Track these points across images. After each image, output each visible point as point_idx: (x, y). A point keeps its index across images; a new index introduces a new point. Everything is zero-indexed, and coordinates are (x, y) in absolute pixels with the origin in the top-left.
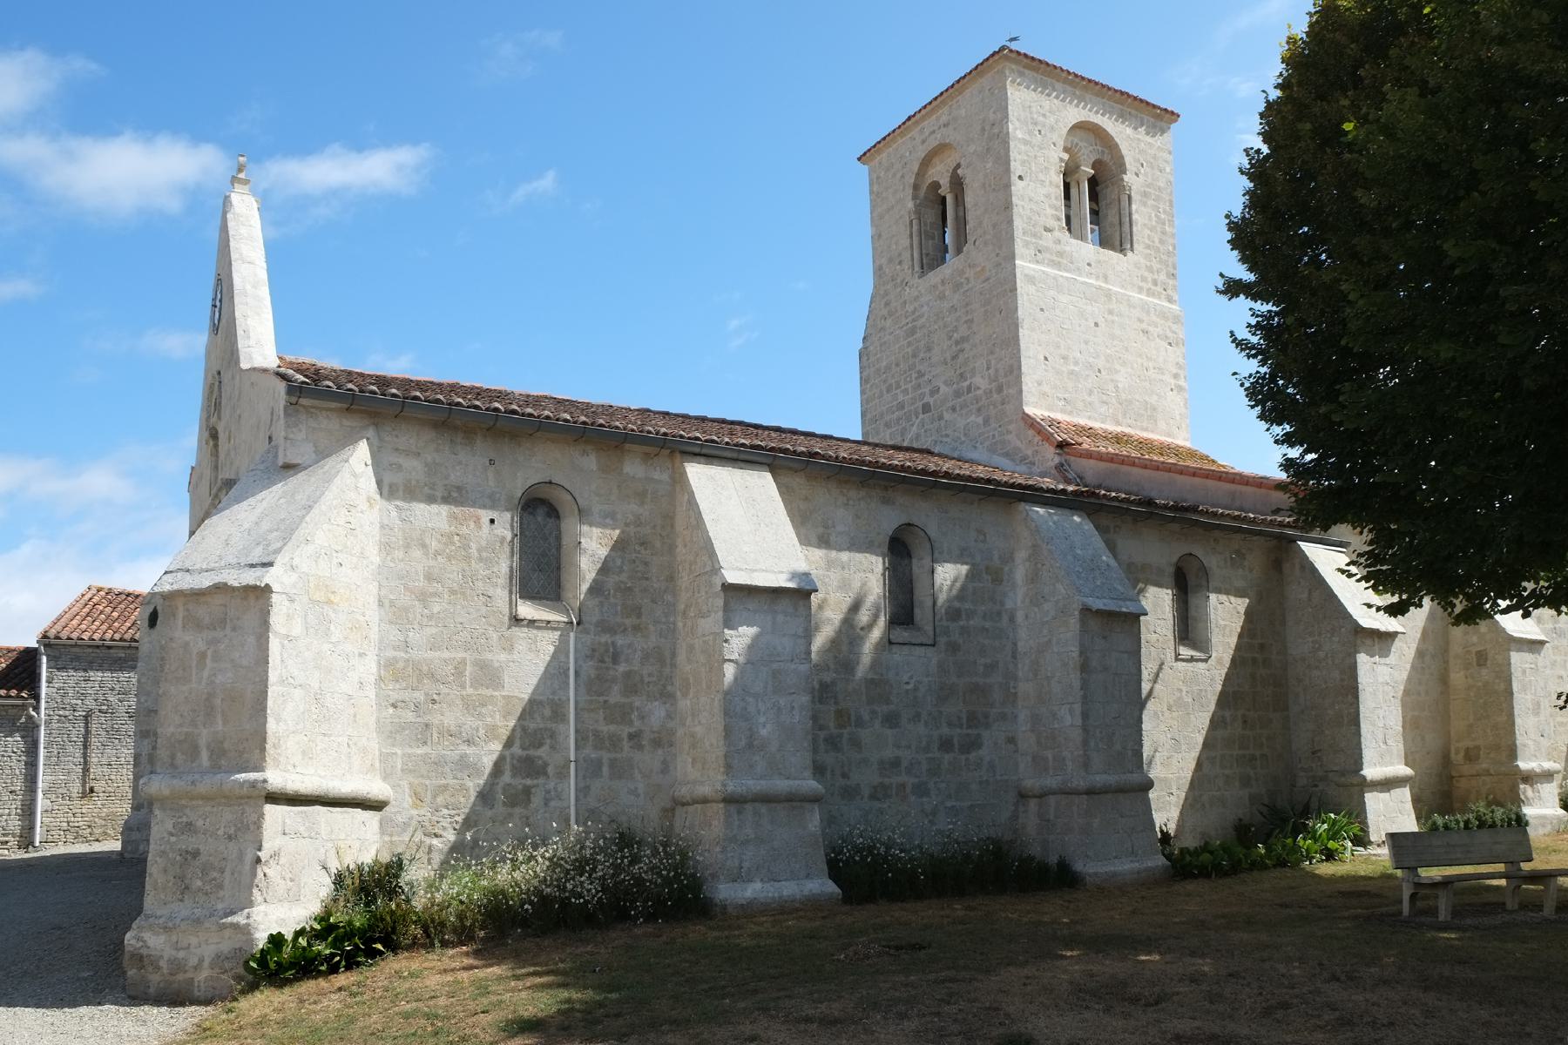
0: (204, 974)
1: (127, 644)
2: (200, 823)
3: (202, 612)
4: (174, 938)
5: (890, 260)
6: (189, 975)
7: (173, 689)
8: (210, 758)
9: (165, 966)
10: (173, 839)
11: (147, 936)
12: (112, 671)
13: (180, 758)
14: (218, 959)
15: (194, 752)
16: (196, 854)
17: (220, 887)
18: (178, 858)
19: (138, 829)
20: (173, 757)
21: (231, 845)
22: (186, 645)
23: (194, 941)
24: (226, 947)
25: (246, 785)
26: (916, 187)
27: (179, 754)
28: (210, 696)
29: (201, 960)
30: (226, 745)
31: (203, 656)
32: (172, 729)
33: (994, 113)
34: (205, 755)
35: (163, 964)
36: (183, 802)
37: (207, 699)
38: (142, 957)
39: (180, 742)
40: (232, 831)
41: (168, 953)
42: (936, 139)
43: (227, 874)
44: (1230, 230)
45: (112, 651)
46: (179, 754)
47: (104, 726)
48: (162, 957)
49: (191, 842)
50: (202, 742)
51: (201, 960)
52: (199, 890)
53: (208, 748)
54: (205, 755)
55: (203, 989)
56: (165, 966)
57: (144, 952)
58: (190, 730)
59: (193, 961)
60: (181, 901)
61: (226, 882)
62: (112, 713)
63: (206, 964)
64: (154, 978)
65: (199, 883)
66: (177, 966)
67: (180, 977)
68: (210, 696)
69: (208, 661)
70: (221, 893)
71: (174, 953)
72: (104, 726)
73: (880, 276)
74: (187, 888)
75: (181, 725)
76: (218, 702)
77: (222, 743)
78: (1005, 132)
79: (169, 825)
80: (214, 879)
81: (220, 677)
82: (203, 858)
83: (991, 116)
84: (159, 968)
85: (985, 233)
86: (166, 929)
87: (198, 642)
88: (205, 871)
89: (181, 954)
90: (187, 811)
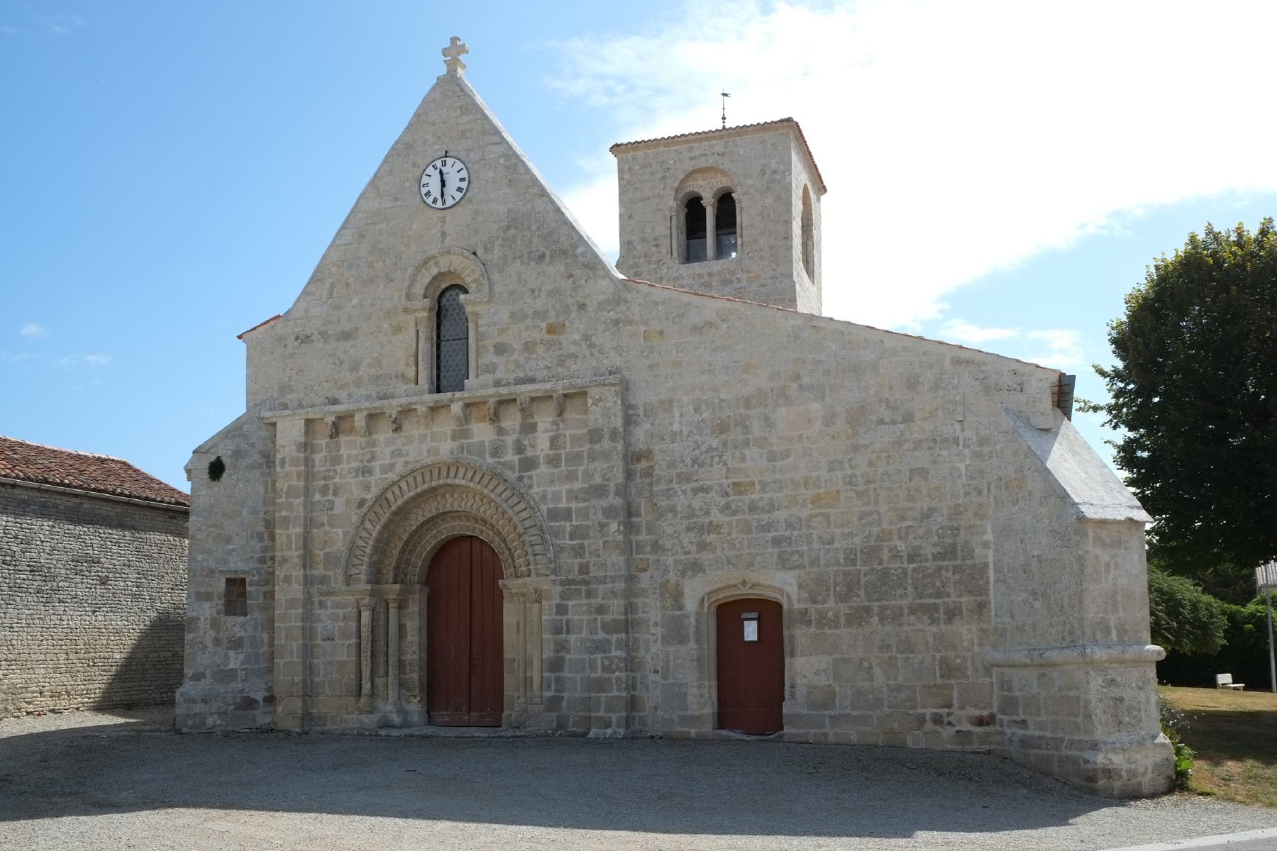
0: (1149, 776)
1: (36, 485)
2: (1119, 679)
3: (1104, 534)
4: (1127, 756)
5: (644, 240)
6: (1138, 780)
7: (1090, 586)
8: (1118, 635)
9: (1125, 775)
10: (1105, 690)
11: (1111, 756)
12: (15, 514)
13: (1099, 635)
14: (1157, 767)
15: (1107, 632)
16: (1121, 700)
17: (1140, 720)
18: (1111, 703)
19: (204, 701)
20: (1094, 634)
21: (1142, 694)
22: (1097, 557)
23: (1138, 756)
24: (1158, 758)
25: (1155, 653)
26: (677, 190)
27: (1098, 632)
28: (1115, 593)
29: (1146, 768)
30: (1127, 627)
31: (1108, 565)
32: (1092, 615)
33: (777, 163)
34: (1114, 633)
35: (1124, 774)
36: (1106, 665)
37: (1113, 595)
38: (1109, 770)
39: (1098, 623)
40: (1140, 684)
41: (1125, 766)
42: (707, 161)
43: (1143, 712)
44: (1112, 343)
45: (17, 491)
46: (1098, 632)
47: (8, 581)
48: (1122, 769)
49: (1117, 692)
50: (1112, 625)
51: (1146, 768)
52: (1129, 723)
53: (1116, 628)
54: (1114, 633)
55: (1148, 787)
56: (1125, 775)
57: (1111, 767)
58: (1104, 615)
59: (1142, 770)
60: (1119, 731)
61: (1143, 718)
62: (15, 566)
63: (1150, 770)
64: (1117, 784)
65: (1127, 719)
66: (1132, 773)
67: (1134, 781)
68: (1115, 593)
69: (1112, 569)
70: (1142, 725)
71: (1128, 765)
72: (8, 581)
73: (629, 249)
74: (1120, 723)
75: (1097, 612)
76: (1119, 597)
77: (1124, 625)
78: (788, 181)
79: (1100, 681)
80: (1136, 716)
81: (1120, 581)
82: (1126, 702)
83: (773, 165)
84: (1121, 777)
85: (760, 250)
86: (1124, 750)
87: (1104, 555)
88: (1129, 710)
89: (1133, 766)
90: (1110, 671)
